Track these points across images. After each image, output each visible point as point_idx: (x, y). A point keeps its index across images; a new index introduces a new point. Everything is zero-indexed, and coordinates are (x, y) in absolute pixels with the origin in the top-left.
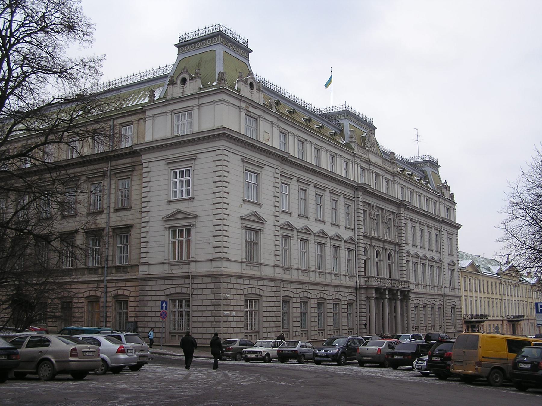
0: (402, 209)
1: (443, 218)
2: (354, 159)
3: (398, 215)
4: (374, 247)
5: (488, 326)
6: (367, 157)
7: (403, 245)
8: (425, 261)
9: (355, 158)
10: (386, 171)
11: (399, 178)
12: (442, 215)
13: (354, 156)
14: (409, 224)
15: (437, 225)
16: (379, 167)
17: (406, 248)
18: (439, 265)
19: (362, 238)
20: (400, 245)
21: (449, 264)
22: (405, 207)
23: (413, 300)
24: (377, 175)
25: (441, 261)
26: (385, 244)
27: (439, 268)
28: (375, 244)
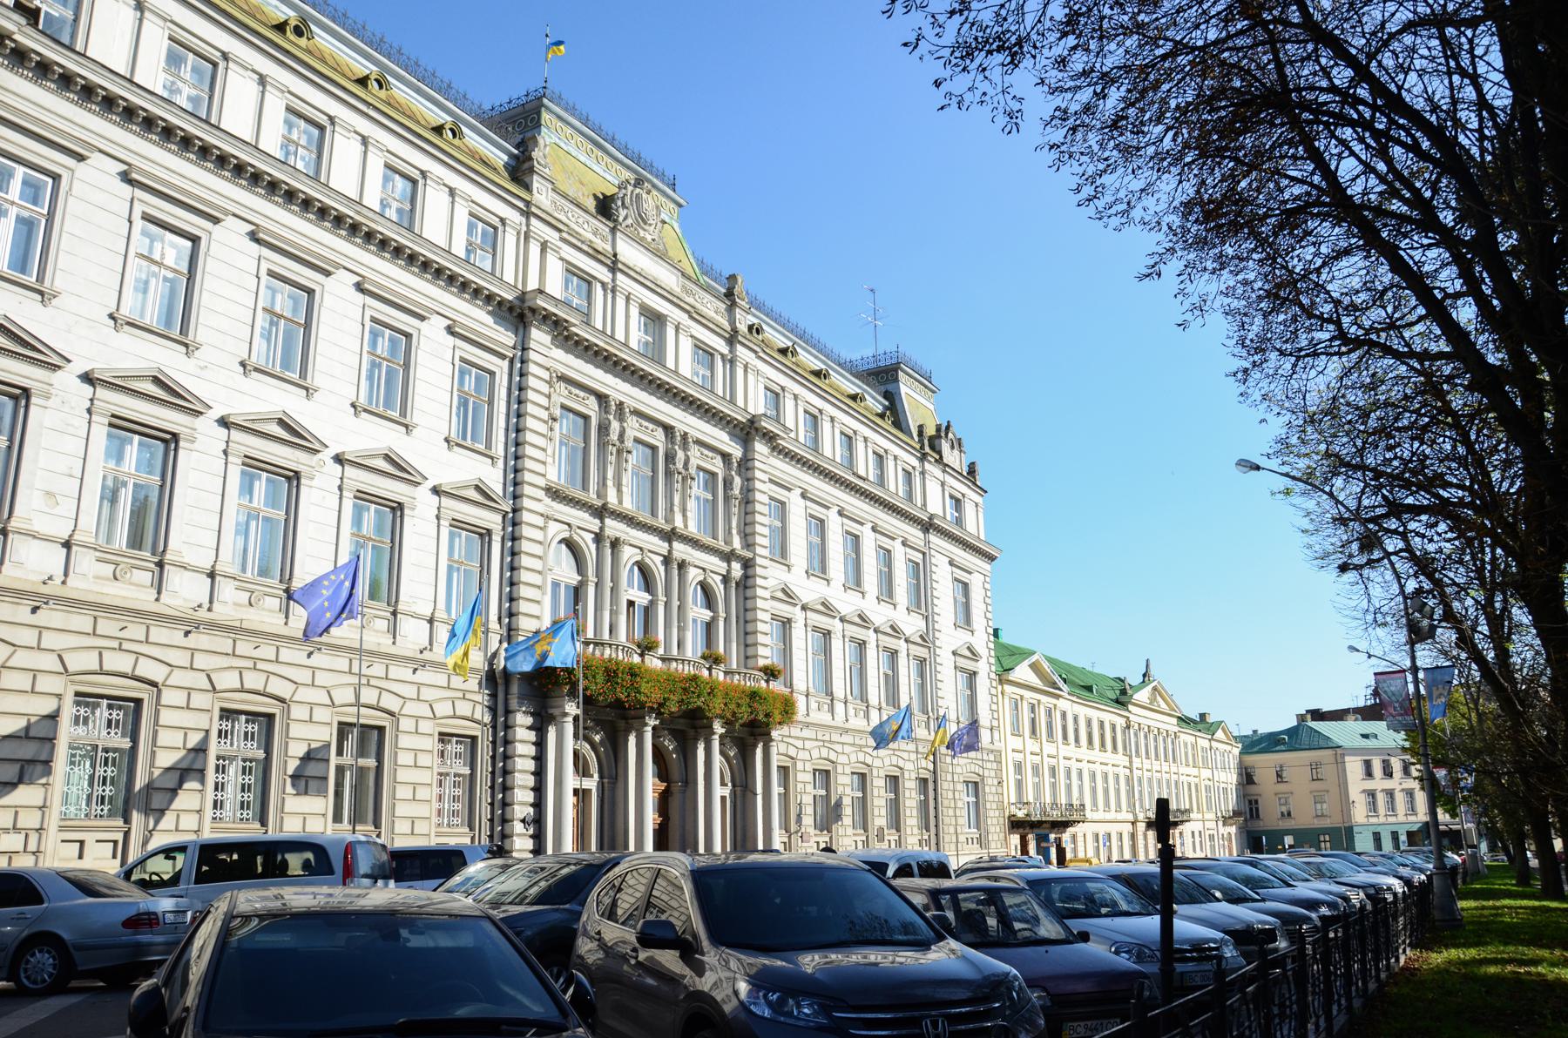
0: (760, 448)
1: (931, 517)
2: (528, 225)
3: (746, 464)
4: (615, 544)
5: (1090, 839)
6: (609, 248)
7: (759, 560)
8: (864, 631)
9: (533, 221)
10: (694, 315)
11: (755, 352)
12: (935, 506)
13: (527, 214)
14: (797, 509)
15: (915, 534)
16: (655, 288)
17: (770, 576)
18: (923, 652)
19: (541, 494)
20: (748, 564)
21: (954, 653)
22: (770, 438)
23: (784, 743)
24: (654, 320)
25: (926, 640)
26: (676, 545)
27: (922, 661)
28: (618, 534)
